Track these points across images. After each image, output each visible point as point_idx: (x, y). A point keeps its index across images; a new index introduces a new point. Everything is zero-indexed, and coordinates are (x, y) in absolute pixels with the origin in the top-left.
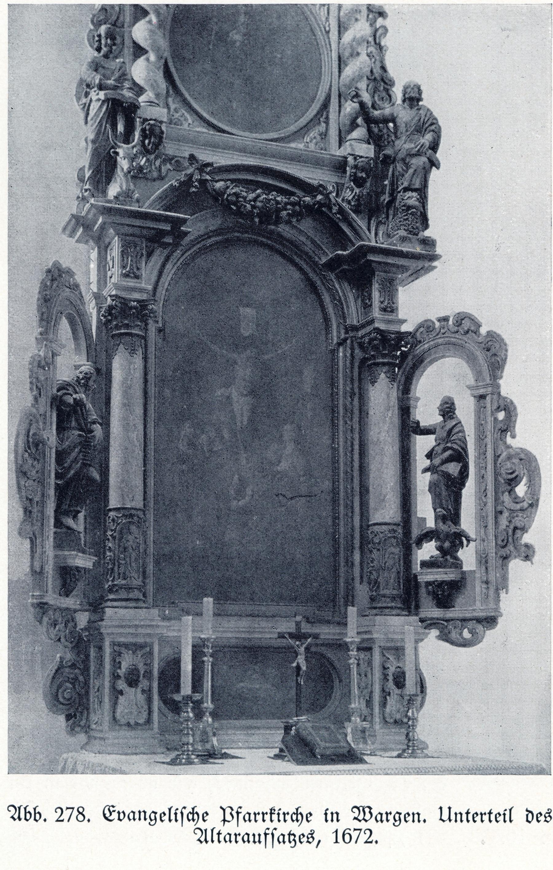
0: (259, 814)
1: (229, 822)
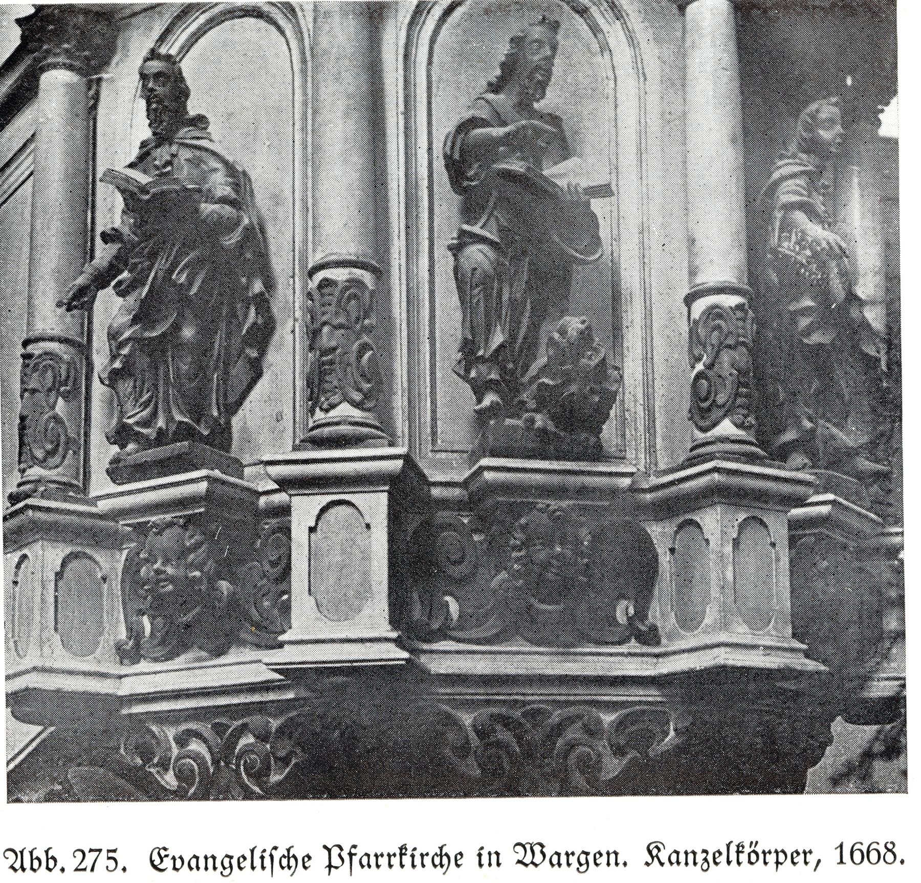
0: (382, 855)
1: (336, 868)
